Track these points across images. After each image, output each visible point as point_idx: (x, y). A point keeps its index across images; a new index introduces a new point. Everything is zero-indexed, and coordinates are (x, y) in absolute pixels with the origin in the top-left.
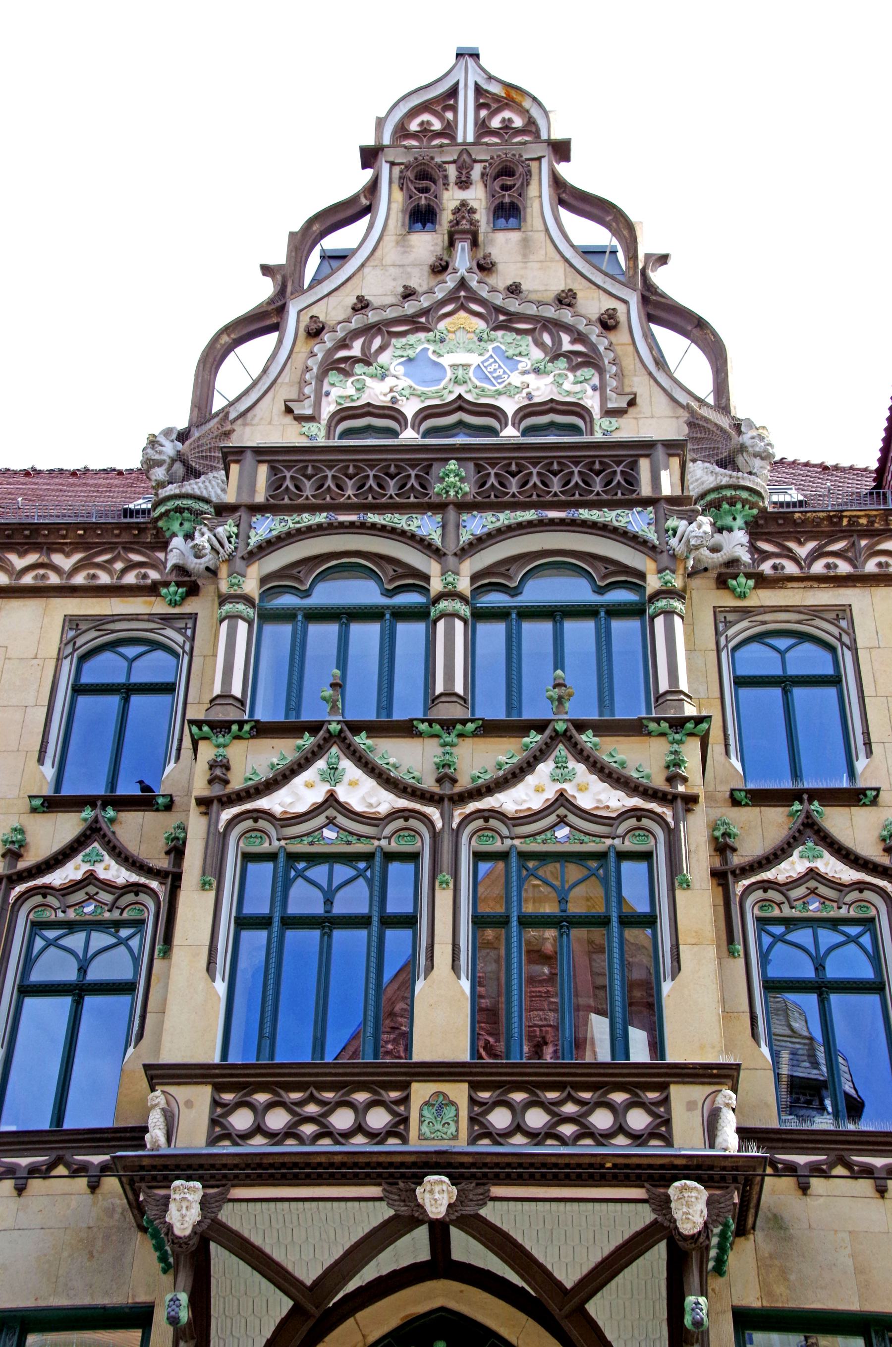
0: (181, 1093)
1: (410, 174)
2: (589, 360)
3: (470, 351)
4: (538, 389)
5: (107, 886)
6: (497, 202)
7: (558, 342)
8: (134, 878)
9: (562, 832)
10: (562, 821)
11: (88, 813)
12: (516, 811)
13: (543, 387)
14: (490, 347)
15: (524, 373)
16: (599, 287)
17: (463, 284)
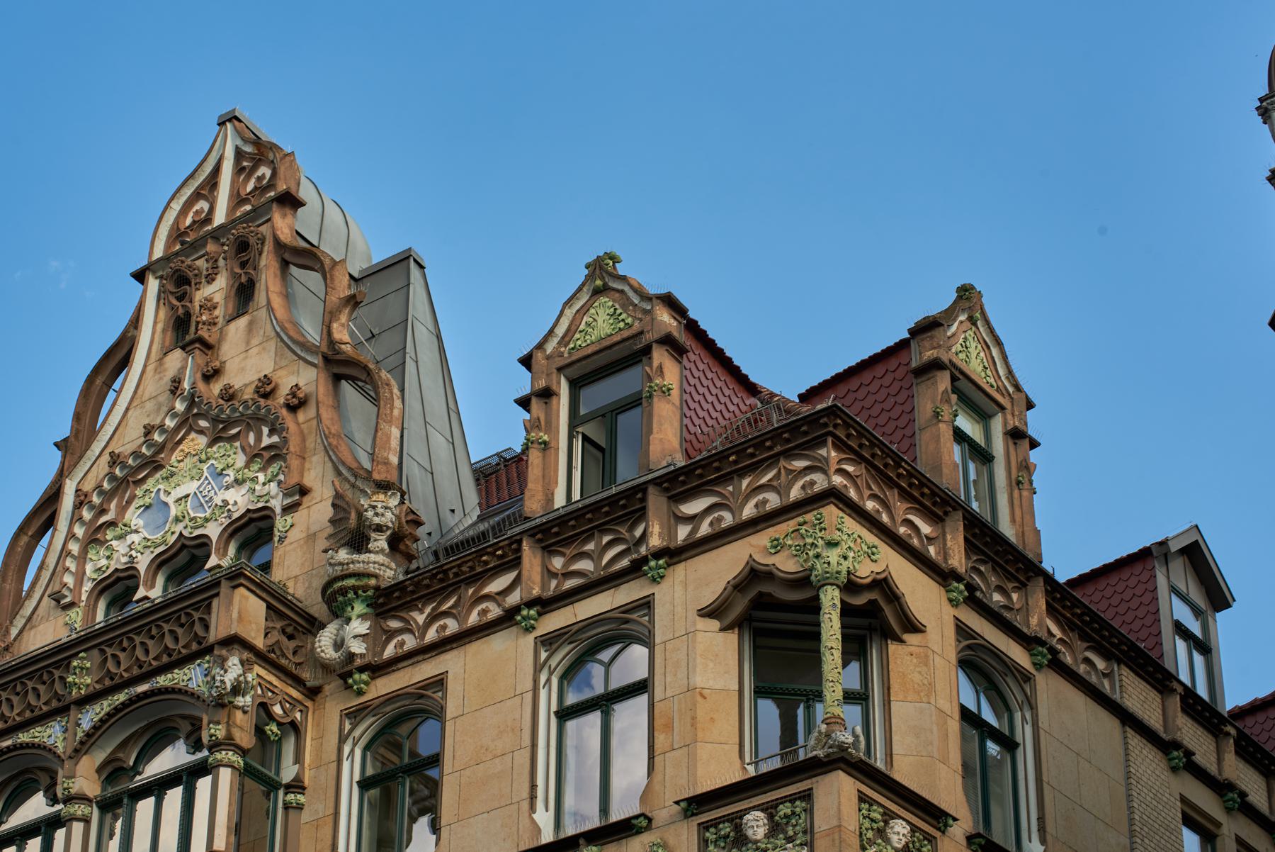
1: (171, 288)
2: (275, 454)
3: (192, 478)
4: (236, 503)
6: (236, 285)
7: (259, 439)
13: (239, 500)
14: (205, 467)
15: (227, 488)
16: (300, 358)
17: (192, 400)
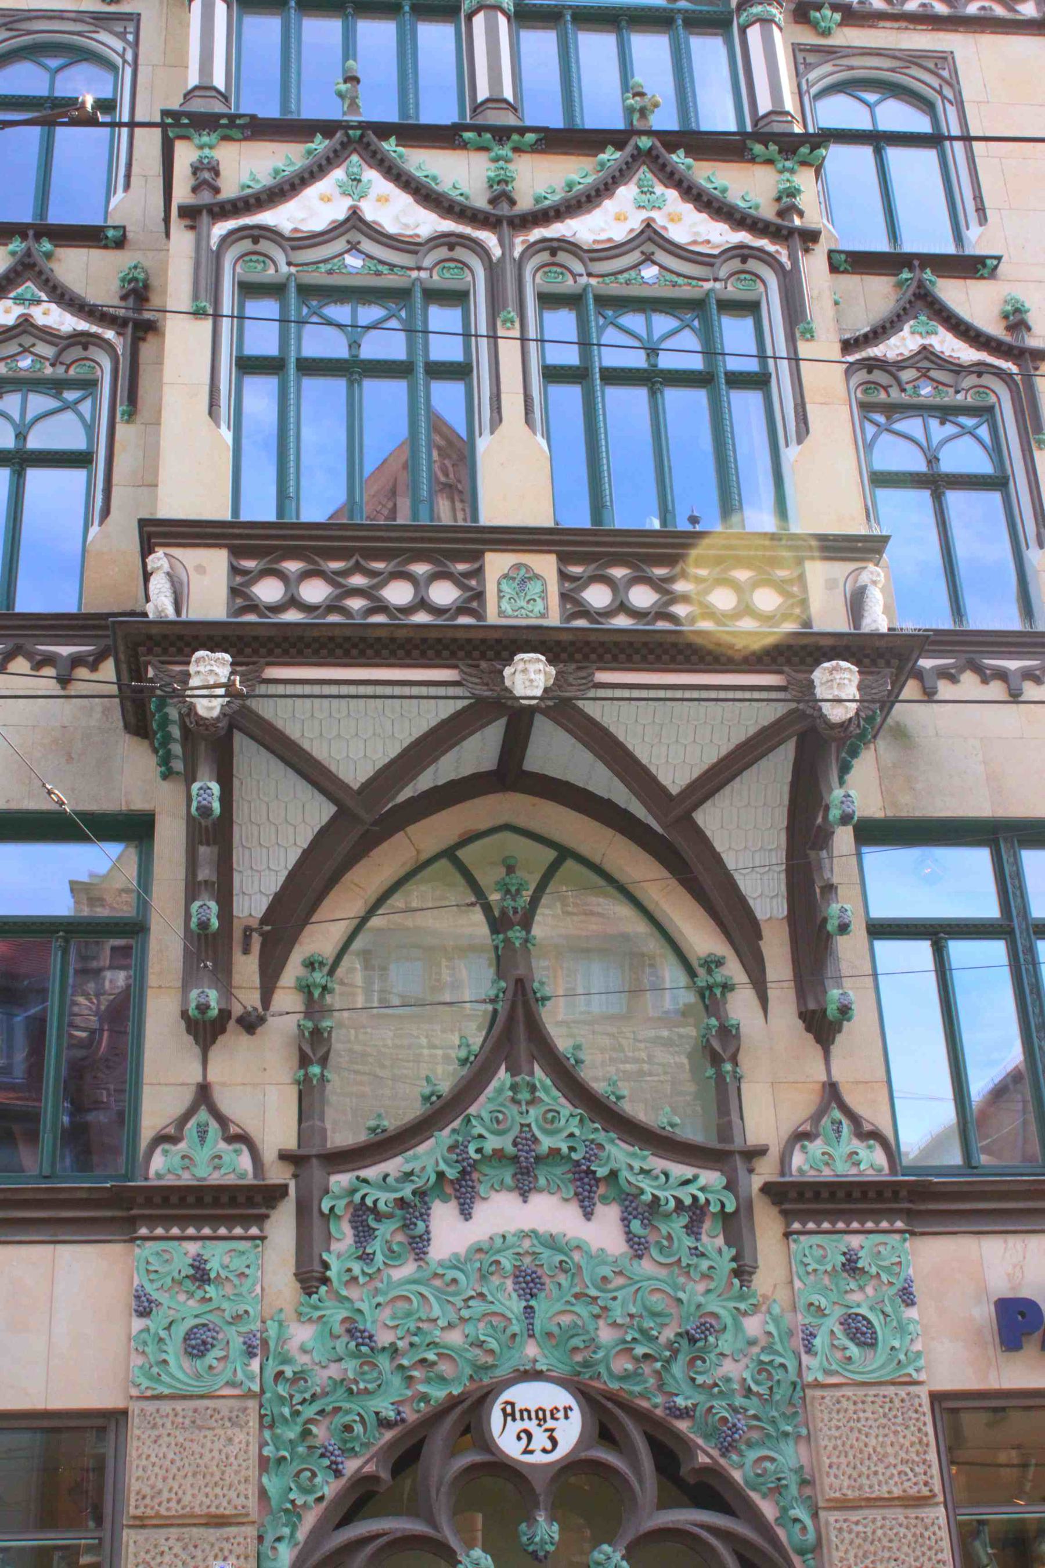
0: (190, 557)
5: (47, 335)
8: (83, 326)
9: (650, 272)
10: (648, 259)
11: (17, 245)
12: (595, 242)
